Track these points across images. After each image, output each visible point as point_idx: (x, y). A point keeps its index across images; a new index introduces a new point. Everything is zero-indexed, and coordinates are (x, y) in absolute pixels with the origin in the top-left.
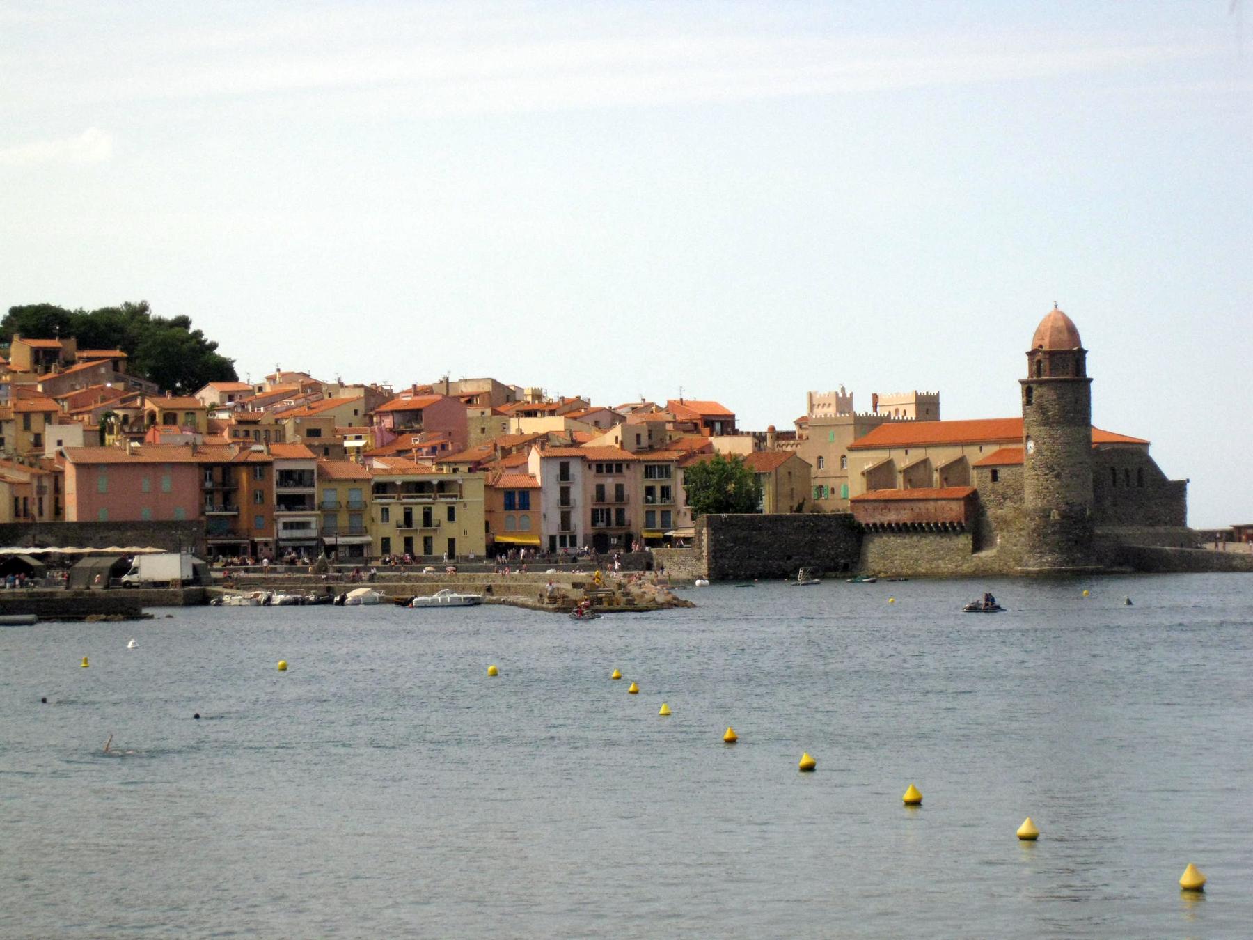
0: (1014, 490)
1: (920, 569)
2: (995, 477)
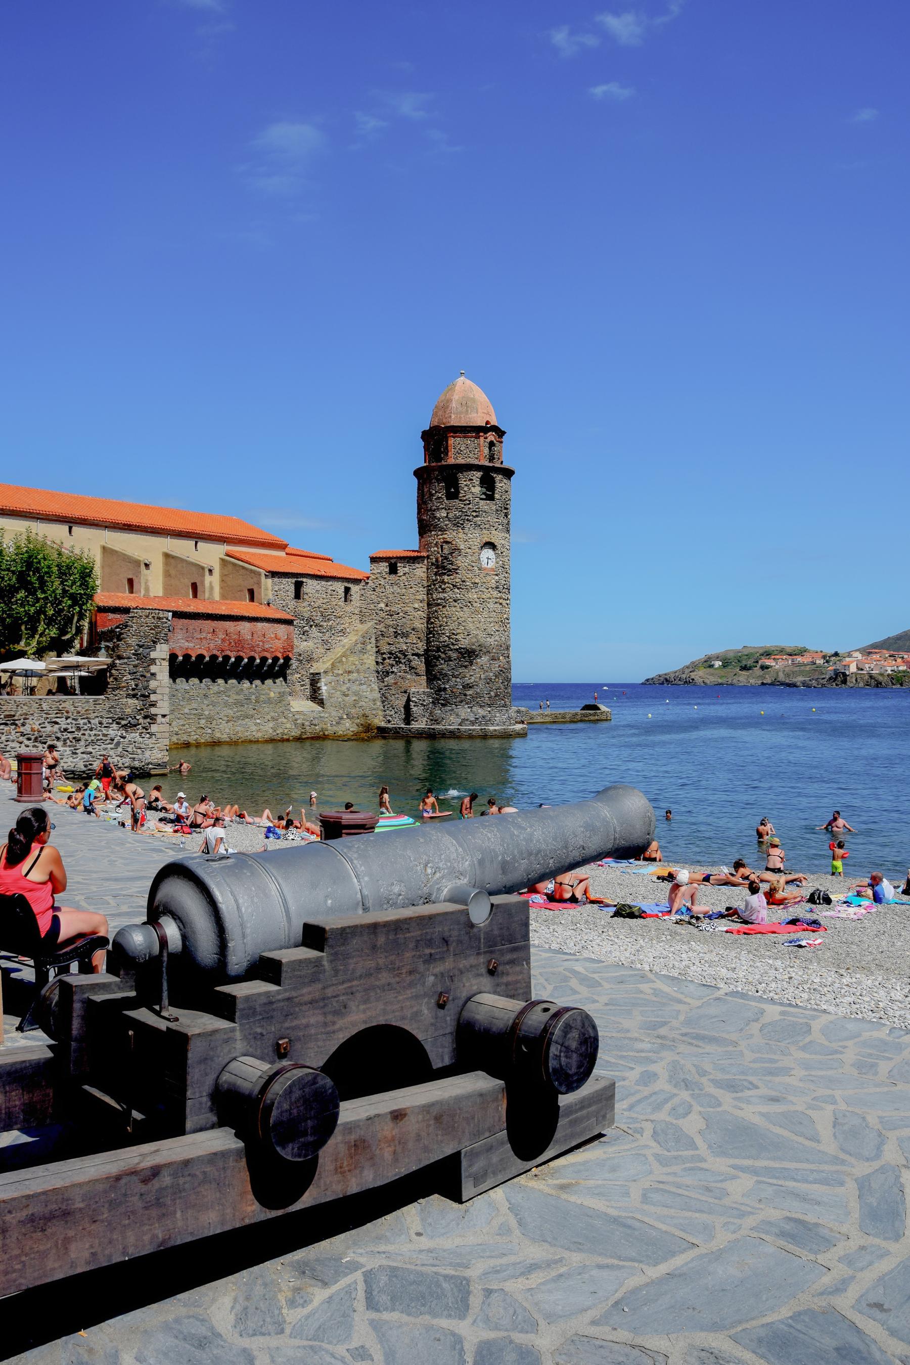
0: (322, 613)
1: (218, 735)
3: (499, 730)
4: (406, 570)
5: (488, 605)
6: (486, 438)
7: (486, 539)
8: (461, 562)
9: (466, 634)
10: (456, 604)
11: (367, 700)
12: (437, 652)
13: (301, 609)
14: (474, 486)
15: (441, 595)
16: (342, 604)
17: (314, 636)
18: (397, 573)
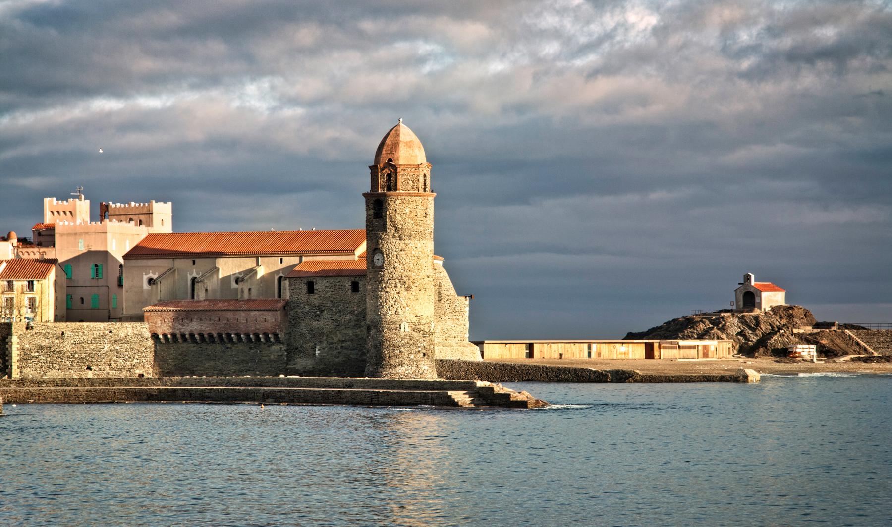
0: (332, 302)
2: (311, 289)
14: (370, 210)
17: (325, 317)
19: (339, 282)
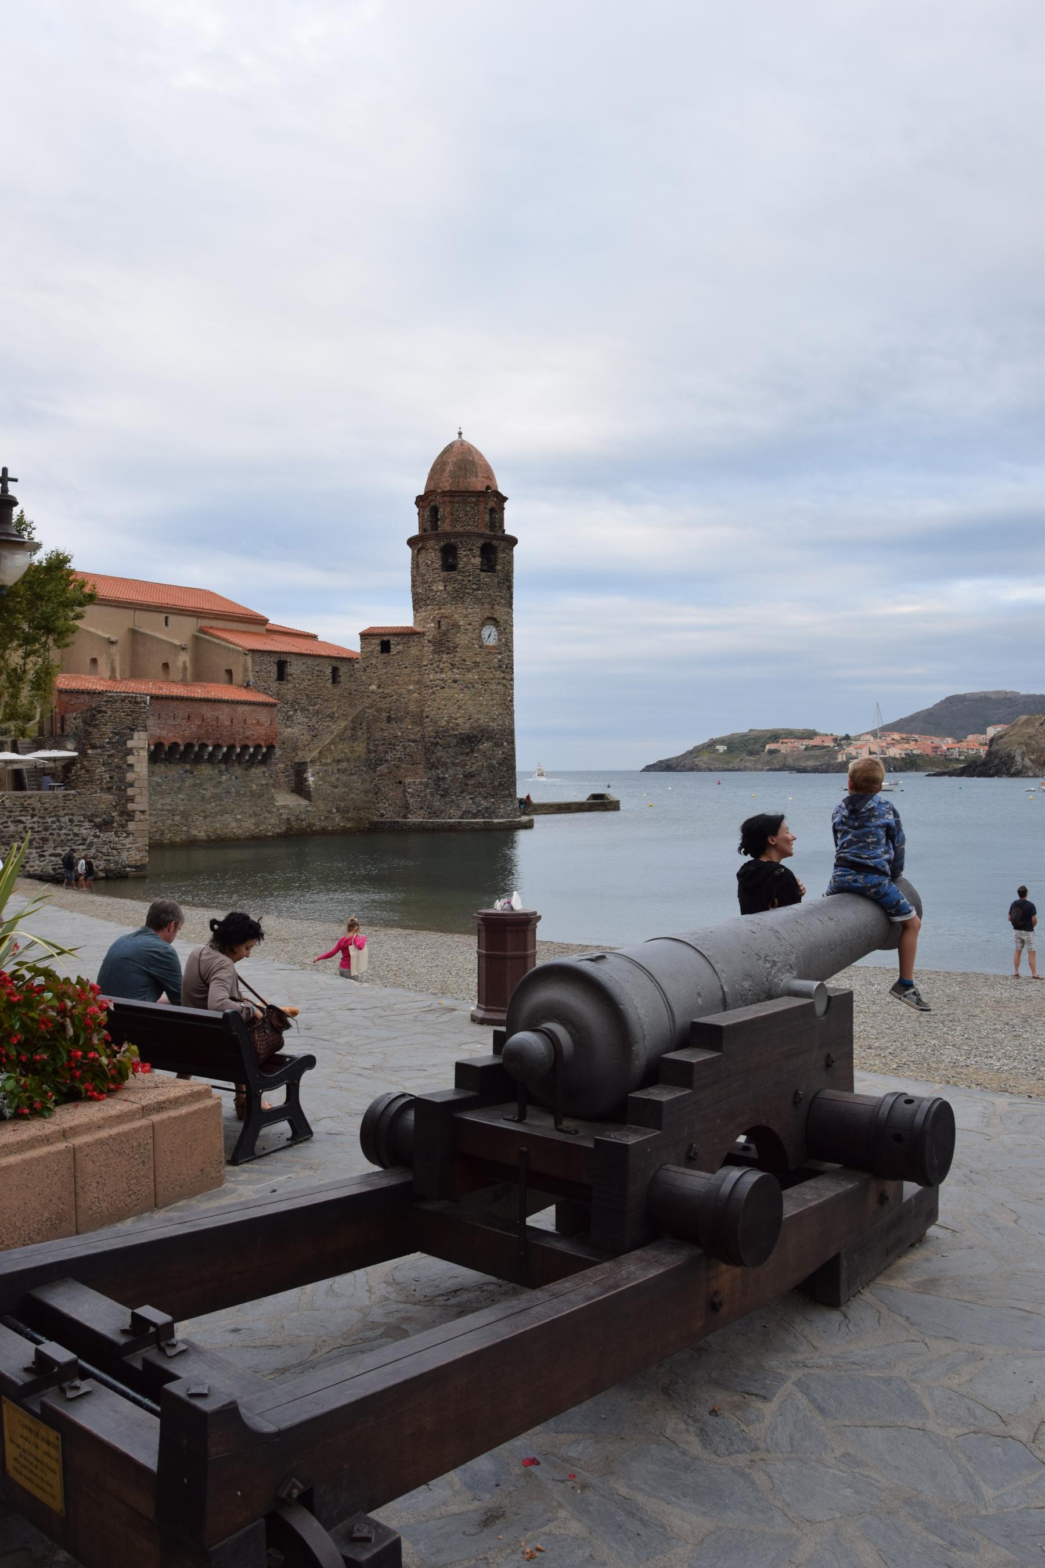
0: (307, 695)
1: (194, 832)
3: (503, 823)
4: (400, 648)
5: (491, 687)
6: (486, 504)
7: (488, 614)
8: (462, 639)
9: (467, 718)
10: (455, 685)
11: (359, 792)
12: (435, 738)
13: (286, 691)
14: (474, 557)
15: (438, 676)
16: (330, 686)
17: (299, 721)
18: (390, 652)
19: (318, 665)
